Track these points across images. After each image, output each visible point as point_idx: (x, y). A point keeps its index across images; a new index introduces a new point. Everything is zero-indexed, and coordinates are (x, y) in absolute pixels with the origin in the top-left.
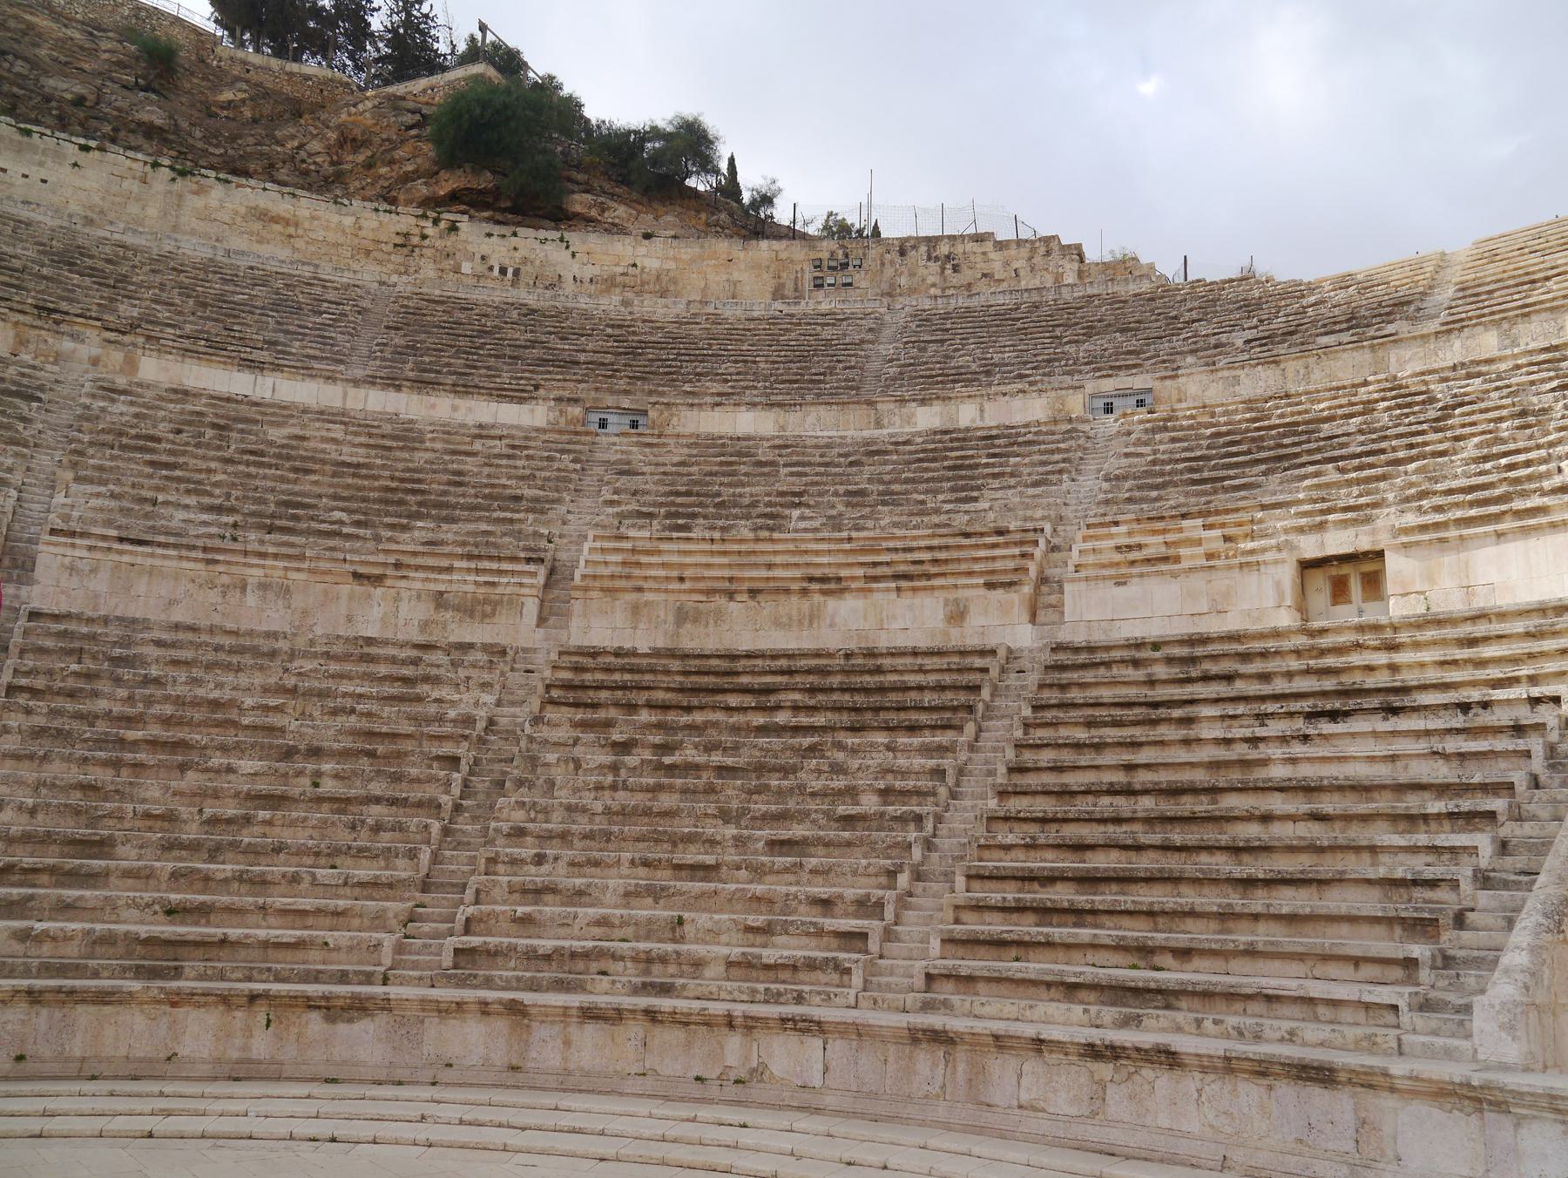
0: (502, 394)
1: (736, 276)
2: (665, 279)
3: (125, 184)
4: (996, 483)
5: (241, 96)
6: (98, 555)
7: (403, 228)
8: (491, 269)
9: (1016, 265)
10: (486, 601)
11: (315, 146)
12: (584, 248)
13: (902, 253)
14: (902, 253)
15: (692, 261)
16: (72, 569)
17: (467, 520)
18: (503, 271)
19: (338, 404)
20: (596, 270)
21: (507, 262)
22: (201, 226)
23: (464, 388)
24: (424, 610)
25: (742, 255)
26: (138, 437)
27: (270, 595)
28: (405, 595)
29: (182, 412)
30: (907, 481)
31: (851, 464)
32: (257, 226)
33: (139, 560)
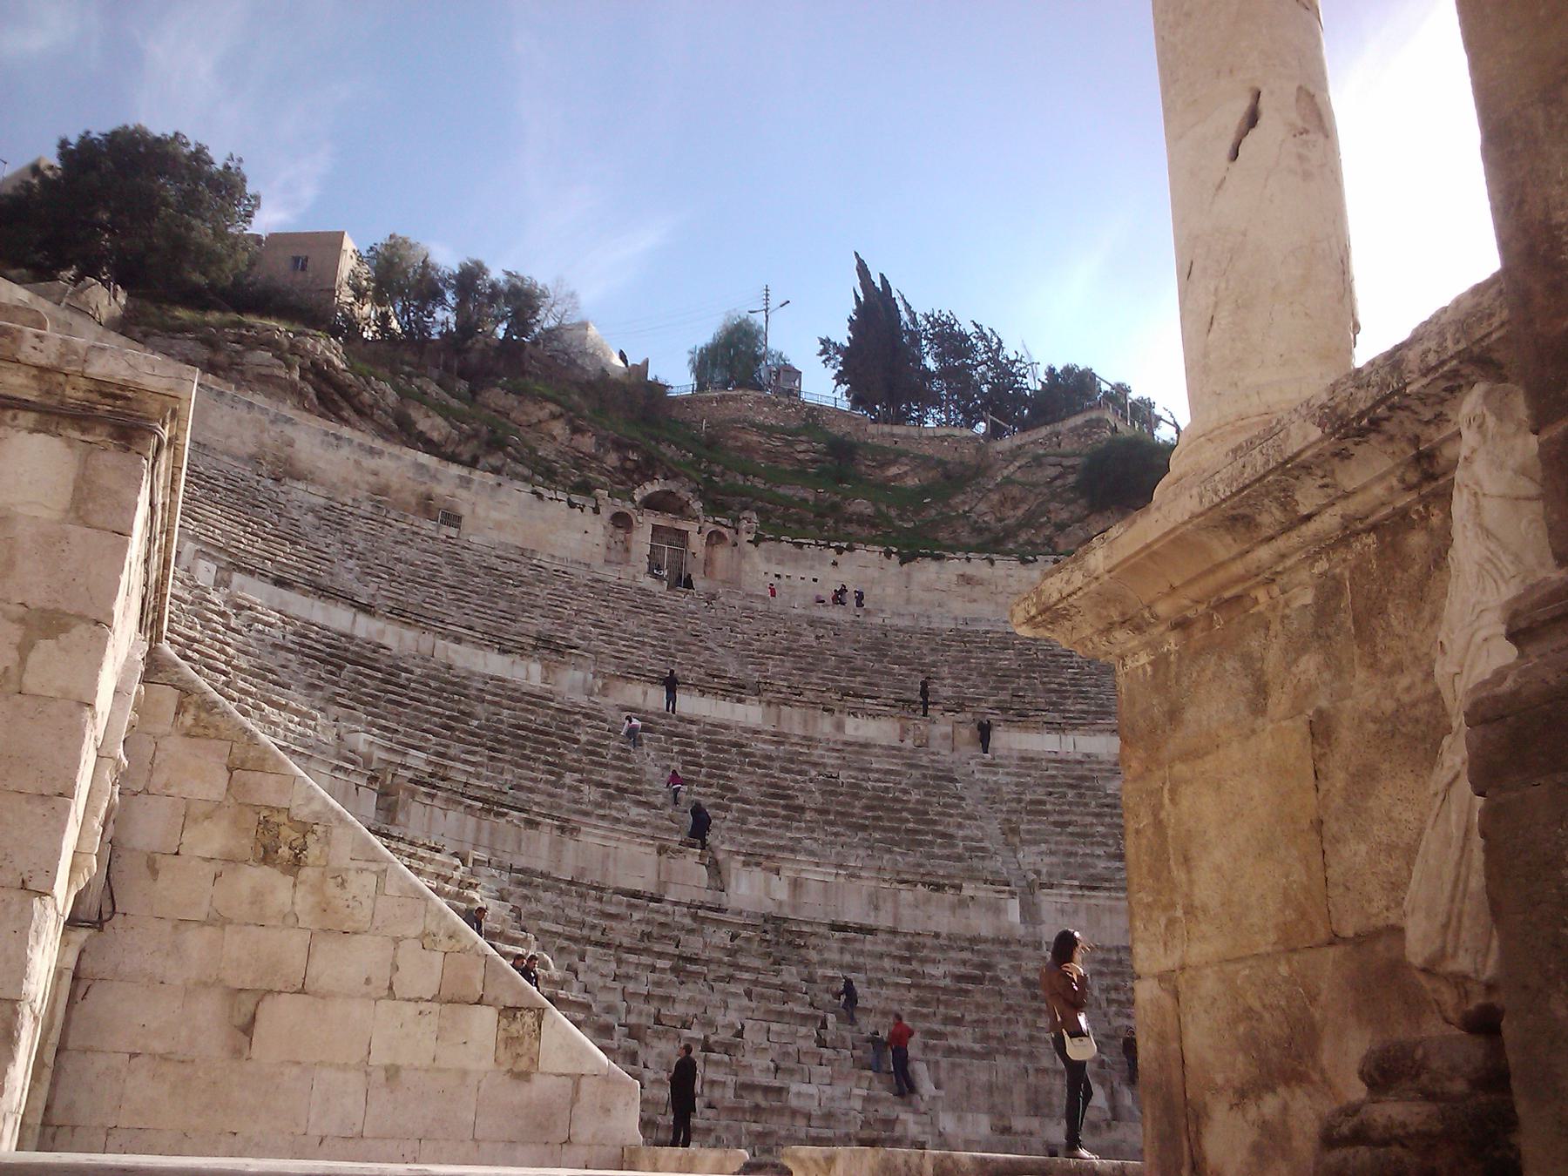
3: (869, 571)
6: (1076, 900)
11: (982, 507)
16: (1062, 912)
22: (926, 596)
26: (1032, 802)
29: (1041, 777)
32: (966, 589)
33: (1101, 902)
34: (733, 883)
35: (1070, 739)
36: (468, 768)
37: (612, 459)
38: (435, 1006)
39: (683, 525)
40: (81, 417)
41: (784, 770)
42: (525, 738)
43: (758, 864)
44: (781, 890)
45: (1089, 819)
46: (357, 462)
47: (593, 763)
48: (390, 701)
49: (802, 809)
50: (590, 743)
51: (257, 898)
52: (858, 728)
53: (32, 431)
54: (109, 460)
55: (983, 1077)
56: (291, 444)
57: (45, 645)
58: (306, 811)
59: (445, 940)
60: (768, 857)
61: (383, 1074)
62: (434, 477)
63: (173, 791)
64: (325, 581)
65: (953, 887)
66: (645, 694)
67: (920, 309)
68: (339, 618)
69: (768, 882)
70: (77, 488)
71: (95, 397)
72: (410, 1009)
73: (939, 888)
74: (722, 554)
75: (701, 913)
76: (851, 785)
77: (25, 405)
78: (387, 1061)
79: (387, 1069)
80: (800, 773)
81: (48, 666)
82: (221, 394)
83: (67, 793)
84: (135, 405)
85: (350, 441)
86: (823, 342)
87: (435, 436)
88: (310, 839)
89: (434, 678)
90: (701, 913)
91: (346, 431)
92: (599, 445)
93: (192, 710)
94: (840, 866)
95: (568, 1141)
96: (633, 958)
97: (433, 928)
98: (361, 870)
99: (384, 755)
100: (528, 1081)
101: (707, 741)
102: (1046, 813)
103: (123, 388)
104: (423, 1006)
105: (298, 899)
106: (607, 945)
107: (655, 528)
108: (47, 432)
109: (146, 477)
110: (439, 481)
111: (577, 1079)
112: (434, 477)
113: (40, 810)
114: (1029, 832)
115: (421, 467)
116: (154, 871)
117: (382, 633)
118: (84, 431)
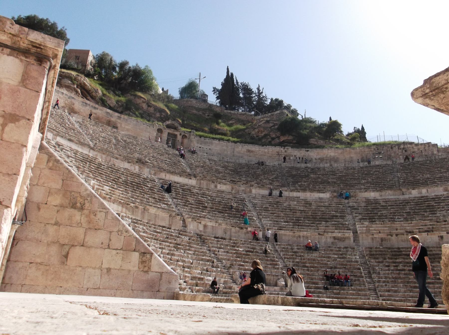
0: (319, 191)
1: (352, 156)
2: (335, 158)
4: (439, 210)
5: (233, 122)
7: (278, 151)
8: (297, 158)
9: (421, 149)
10: (343, 238)
11: (253, 133)
12: (317, 152)
13: (392, 148)
14: (392, 148)
15: (341, 153)
17: (330, 221)
18: (300, 158)
19: (288, 196)
20: (320, 157)
21: (300, 156)
23: (312, 191)
24: (332, 240)
25: (353, 151)
26: (265, 208)
27: (305, 238)
28: (328, 237)
30: (418, 209)
31: (403, 205)
32: (249, 153)
34: (189, 225)
36: (120, 192)
37: (158, 115)
38: (122, 251)
39: (176, 133)
40: (25, 52)
41: (201, 197)
42: (135, 185)
43: (195, 221)
44: (201, 228)
45: (280, 213)
47: (152, 193)
48: (99, 173)
49: (206, 207)
50: (151, 187)
51: (70, 218)
52: (220, 187)
53: (8, 55)
54: (34, 68)
56: (74, 105)
57: (10, 126)
58: (85, 193)
59: (124, 233)
60: (198, 219)
61: (106, 270)
62: (111, 116)
63: (46, 185)
64: (82, 141)
65: (245, 228)
66: (166, 175)
67: (240, 81)
68: (85, 151)
69: (198, 225)
70: (23, 75)
71: (30, 47)
72: (114, 252)
73: (242, 228)
74: (186, 141)
75: (181, 233)
76: (219, 202)
77: (6, 46)
78: (107, 267)
79: (107, 269)
80: (206, 198)
81: (11, 132)
83: (17, 174)
84: (43, 51)
85: (89, 105)
86: (214, 88)
87: (112, 105)
88: (86, 201)
89: (110, 168)
90: (181, 233)
91: (88, 102)
93: (52, 162)
94: (216, 222)
95: (159, 291)
96: (164, 243)
97: (121, 229)
98: (100, 211)
99: (98, 187)
100: (148, 274)
101: (182, 188)
102: (269, 211)
103: (40, 45)
104: (118, 251)
105: (82, 219)
106: (157, 240)
107: (169, 133)
108: (14, 56)
109: (46, 76)
110: (112, 117)
111: (161, 273)
112: (111, 116)
113: (7, 179)
114: (264, 215)
115: (108, 113)
116: (39, 209)
117: (97, 155)
118: (26, 57)
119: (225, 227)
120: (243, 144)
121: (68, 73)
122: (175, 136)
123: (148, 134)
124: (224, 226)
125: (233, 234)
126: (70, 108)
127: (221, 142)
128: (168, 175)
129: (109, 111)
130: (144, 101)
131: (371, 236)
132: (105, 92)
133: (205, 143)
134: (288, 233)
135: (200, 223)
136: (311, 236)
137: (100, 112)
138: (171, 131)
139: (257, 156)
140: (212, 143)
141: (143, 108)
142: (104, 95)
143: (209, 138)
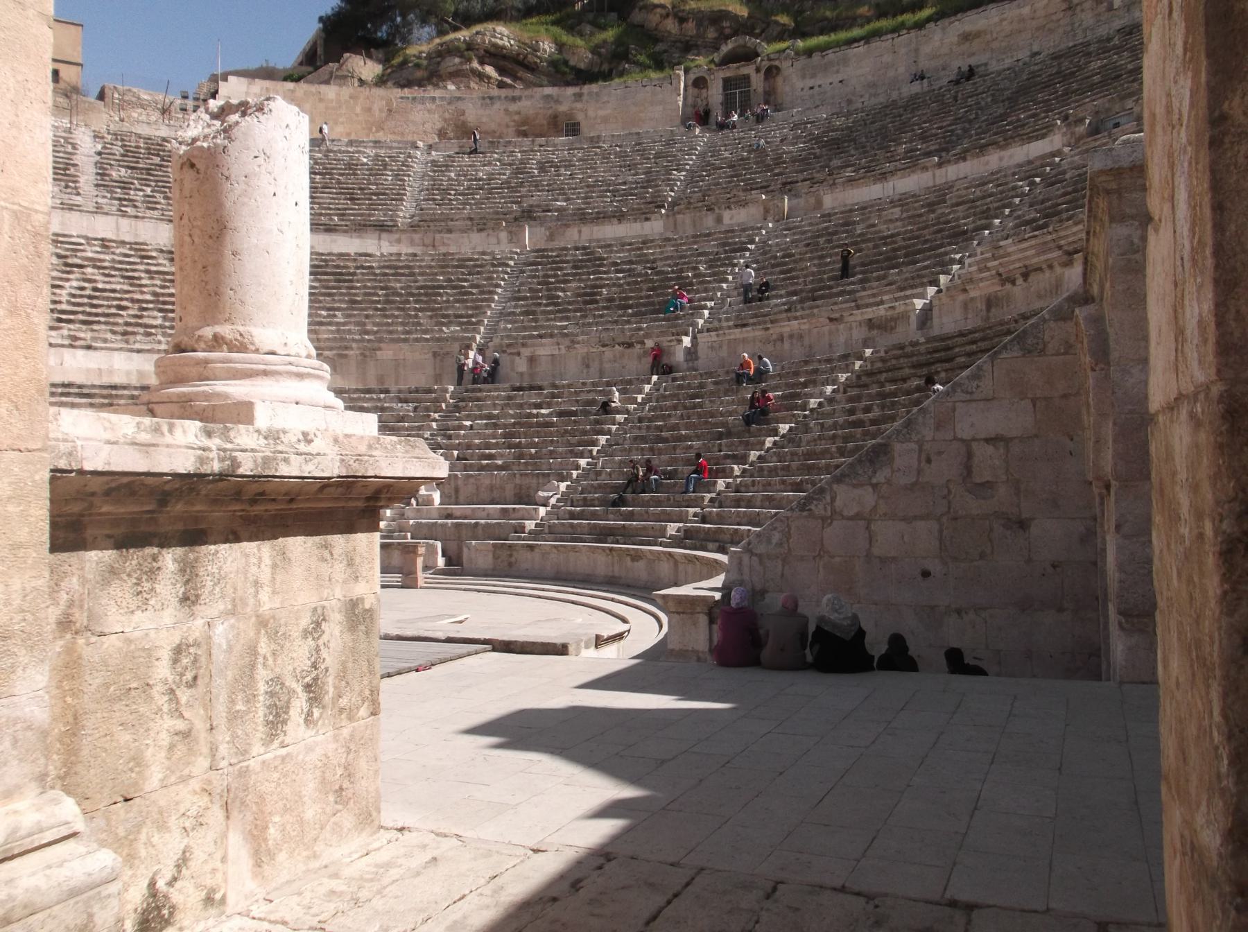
16: (712, 348)
19: (931, 184)
28: (854, 325)
35: (891, 184)
37: (711, 34)
46: (506, 110)
55: (487, 482)
56: (463, 114)
62: (557, 102)
66: (580, 232)
69: (513, 362)
73: (630, 345)
82: (414, 99)
85: (499, 97)
87: (582, 66)
92: (699, 24)
107: (727, 83)
115: (548, 97)
119: (586, 350)
120: (946, 21)
121: (451, 41)
122: (747, 78)
123: (660, 108)
124: (581, 350)
125: (607, 366)
126: (456, 126)
127: (876, 44)
128: (586, 230)
129: (548, 90)
130: (663, 12)
131: (961, 297)
132: (566, 38)
133: (825, 68)
134: (751, 334)
135: (519, 354)
136: (810, 330)
137: (528, 103)
138: (731, 71)
139: (995, 45)
140: (845, 61)
141: (669, 32)
142: (560, 46)
143: (838, 44)
